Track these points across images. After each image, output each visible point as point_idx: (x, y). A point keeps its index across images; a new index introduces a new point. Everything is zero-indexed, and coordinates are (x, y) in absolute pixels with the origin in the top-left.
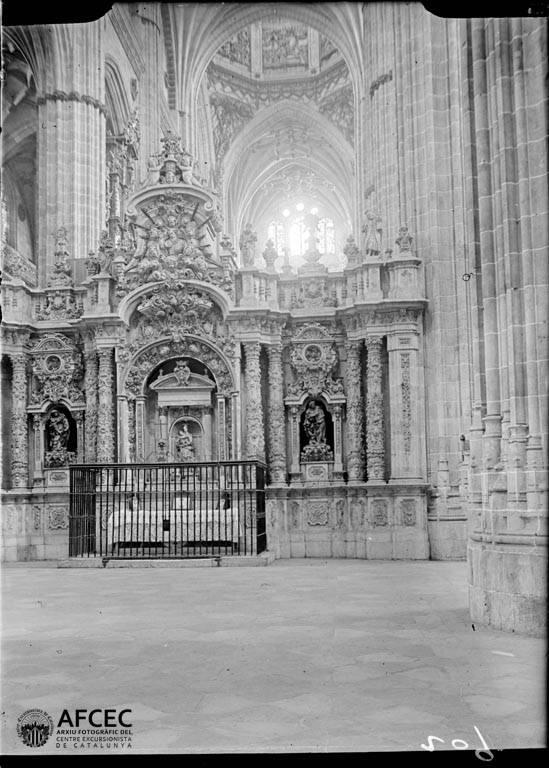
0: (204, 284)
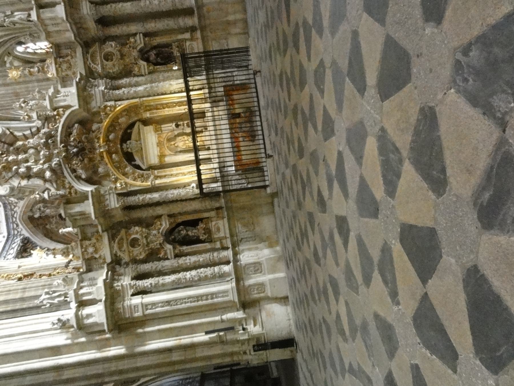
0: (60, 129)
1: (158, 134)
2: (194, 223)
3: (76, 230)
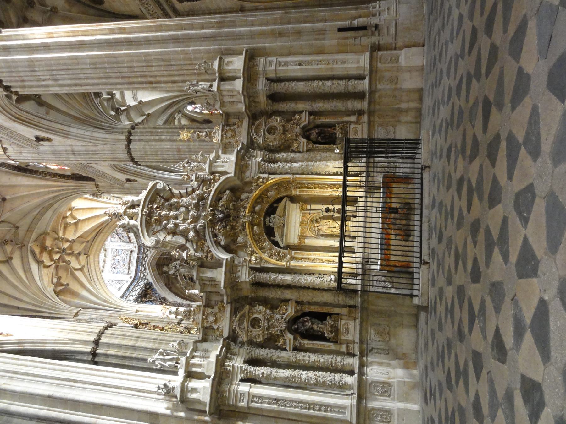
1: (303, 213)
2: (322, 317)
3: (202, 294)
